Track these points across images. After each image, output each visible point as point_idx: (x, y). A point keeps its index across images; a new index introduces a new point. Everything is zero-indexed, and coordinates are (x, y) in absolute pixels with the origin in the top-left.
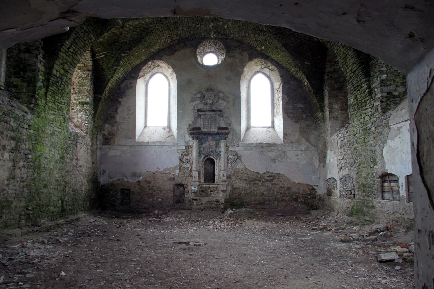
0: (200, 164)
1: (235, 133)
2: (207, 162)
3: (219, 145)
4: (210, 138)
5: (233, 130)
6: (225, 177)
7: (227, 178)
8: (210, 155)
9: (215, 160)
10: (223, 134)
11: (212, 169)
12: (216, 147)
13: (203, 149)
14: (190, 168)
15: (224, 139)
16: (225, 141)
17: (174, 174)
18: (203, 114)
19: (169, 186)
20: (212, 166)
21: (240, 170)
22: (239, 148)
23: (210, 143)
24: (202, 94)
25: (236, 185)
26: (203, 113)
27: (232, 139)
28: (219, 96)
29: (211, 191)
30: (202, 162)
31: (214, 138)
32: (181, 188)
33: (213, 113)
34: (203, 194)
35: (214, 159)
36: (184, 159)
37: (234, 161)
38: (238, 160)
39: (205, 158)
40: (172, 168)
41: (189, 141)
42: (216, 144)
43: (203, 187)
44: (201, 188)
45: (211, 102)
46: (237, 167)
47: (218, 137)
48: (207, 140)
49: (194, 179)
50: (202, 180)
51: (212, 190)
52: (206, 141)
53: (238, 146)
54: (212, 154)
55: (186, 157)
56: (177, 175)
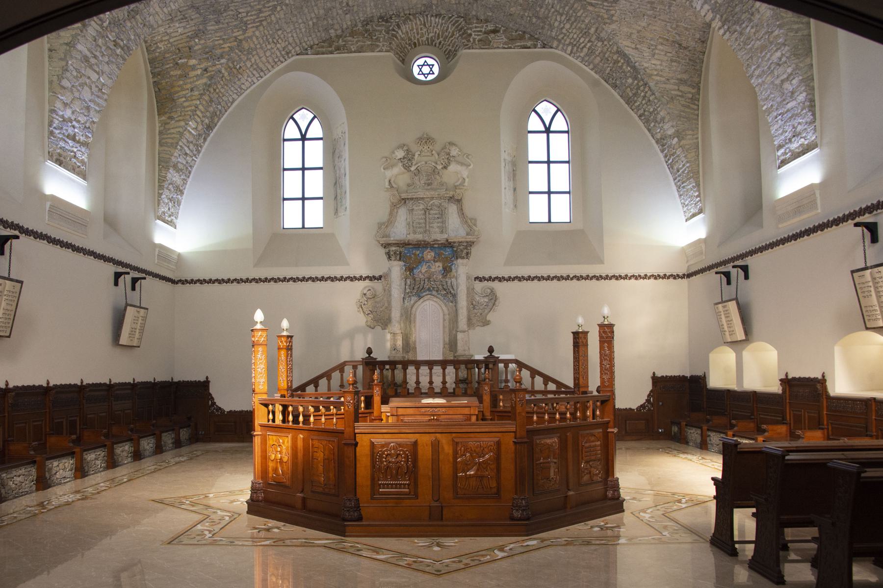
3: (451, 270)
4: (429, 255)
12: (444, 276)
15: (463, 258)
16: (465, 261)
23: (429, 267)
24: (408, 151)
28: (449, 154)
31: (439, 255)
42: (445, 269)
47: (448, 252)
52: (420, 262)
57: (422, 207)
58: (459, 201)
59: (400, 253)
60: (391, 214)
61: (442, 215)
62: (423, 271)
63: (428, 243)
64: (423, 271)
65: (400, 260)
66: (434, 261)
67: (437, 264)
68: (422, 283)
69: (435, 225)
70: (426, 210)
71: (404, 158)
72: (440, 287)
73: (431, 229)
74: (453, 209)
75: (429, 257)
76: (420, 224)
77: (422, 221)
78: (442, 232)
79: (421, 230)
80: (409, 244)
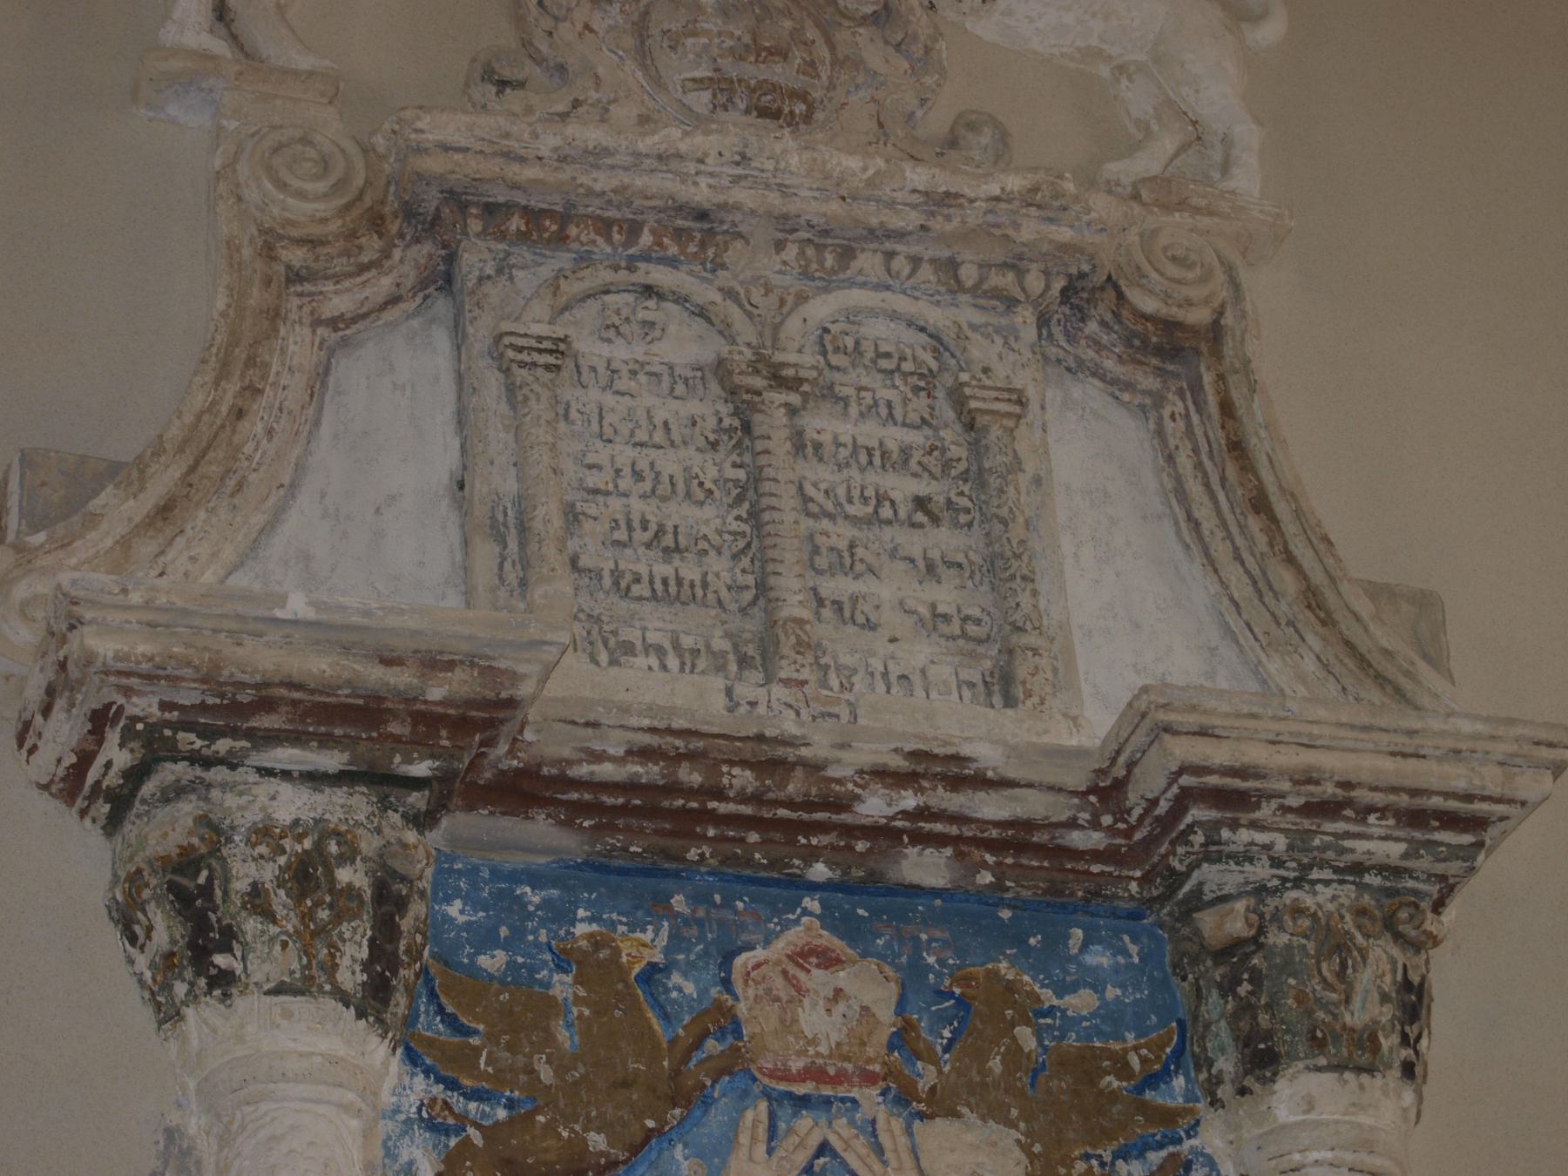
15: (1357, 1055)
31: (978, 1013)
47: (1092, 984)
52: (684, 1095)
57: (685, 344)
58: (1182, 357)
59: (388, 898)
60: (241, 359)
61: (973, 476)
65: (374, 999)
66: (903, 1097)
69: (887, 591)
70: (750, 392)
73: (842, 644)
74: (1089, 455)
75: (821, 1025)
76: (667, 543)
77: (707, 519)
78: (1003, 687)
79: (696, 626)
80: (524, 790)
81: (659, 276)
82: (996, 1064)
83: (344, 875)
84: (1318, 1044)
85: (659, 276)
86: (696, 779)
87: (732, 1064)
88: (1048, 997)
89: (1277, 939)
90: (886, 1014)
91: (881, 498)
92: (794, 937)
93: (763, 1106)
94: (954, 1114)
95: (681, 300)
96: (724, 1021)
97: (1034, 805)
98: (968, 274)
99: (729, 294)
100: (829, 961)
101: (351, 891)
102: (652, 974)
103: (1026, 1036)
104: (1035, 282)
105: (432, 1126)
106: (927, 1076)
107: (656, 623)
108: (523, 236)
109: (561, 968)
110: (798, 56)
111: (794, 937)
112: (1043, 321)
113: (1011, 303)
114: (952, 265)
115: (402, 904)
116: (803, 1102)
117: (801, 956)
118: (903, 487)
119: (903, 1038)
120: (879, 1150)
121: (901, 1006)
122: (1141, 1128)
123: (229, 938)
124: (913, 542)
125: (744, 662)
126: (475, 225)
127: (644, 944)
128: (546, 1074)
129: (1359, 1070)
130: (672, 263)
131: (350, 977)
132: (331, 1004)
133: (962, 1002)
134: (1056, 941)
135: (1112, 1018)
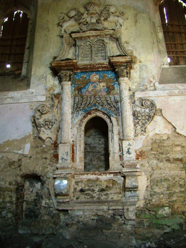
0: (75, 130)
1: (144, 68)
2: (92, 131)
4: (95, 77)
5: (140, 62)
6: (133, 156)
7: (137, 159)
8: (97, 110)
9: (108, 121)
10: (121, 64)
11: (103, 146)
12: (108, 92)
13: (80, 99)
14: (54, 139)
15: (124, 76)
16: (126, 79)
17: (20, 152)
18: (81, 38)
19: (9, 179)
20: (103, 140)
21: (165, 138)
22: (156, 92)
23: (95, 87)
25: (157, 175)
26: (78, 35)
27: (140, 77)
28: (109, 10)
29: (102, 190)
30: (80, 125)
32: (38, 185)
33: (98, 33)
34: (83, 198)
35: (104, 117)
36: (41, 121)
37: (150, 118)
38: (158, 118)
39: (85, 117)
40: (17, 140)
41: (54, 86)
42: (108, 87)
43: (82, 181)
44: (77, 183)
45: (94, 21)
46: (157, 131)
48: (88, 82)
49: (60, 161)
50: (79, 164)
51: (104, 187)
53: (155, 89)
54: (100, 108)
55: (45, 117)
56: (25, 156)
62: (90, 90)
63: (94, 67)
64: (90, 90)
67: (102, 84)
68: (89, 99)
71: (75, 15)
72: (105, 102)
75: (95, 79)
76: (87, 54)
81: (87, 40)
82: (105, 80)
83: (67, 75)
84: (121, 76)
85: (87, 40)
86: (86, 67)
87: (90, 82)
88: (108, 76)
89: (119, 70)
90: (98, 78)
91: (99, 50)
92: (94, 74)
93: (91, 84)
94: (102, 82)
95: (88, 41)
96: (90, 80)
97: (105, 65)
98: (104, 36)
99: (91, 40)
100: (95, 75)
101: (68, 76)
102: (86, 78)
103: (106, 78)
104: (108, 36)
105: (74, 87)
106: (101, 81)
107: (86, 59)
108: (79, 40)
109: (81, 78)
110: (95, 26)
111: (94, 74)
112: (109, 38)
113: (107, 38)
114: (103, 36)
115: (71, 76)
116: (94, 83)
117: (94, 75)
118: (100, 49)
119: (99, 79)
120: (98, 85)
121: (99, 77)
122: (113, 82)
123: (62, 79)
124: (100, 52)
125: (90, 60)
126: (77, 39)
127: (85, 76)
128: (80, 83)
129: (124, 77)
130: (88, 39)
131: (68, 80)
132: (67, 81)
133: (103, 77)
134: (108, 73)
135: (111, 76)
